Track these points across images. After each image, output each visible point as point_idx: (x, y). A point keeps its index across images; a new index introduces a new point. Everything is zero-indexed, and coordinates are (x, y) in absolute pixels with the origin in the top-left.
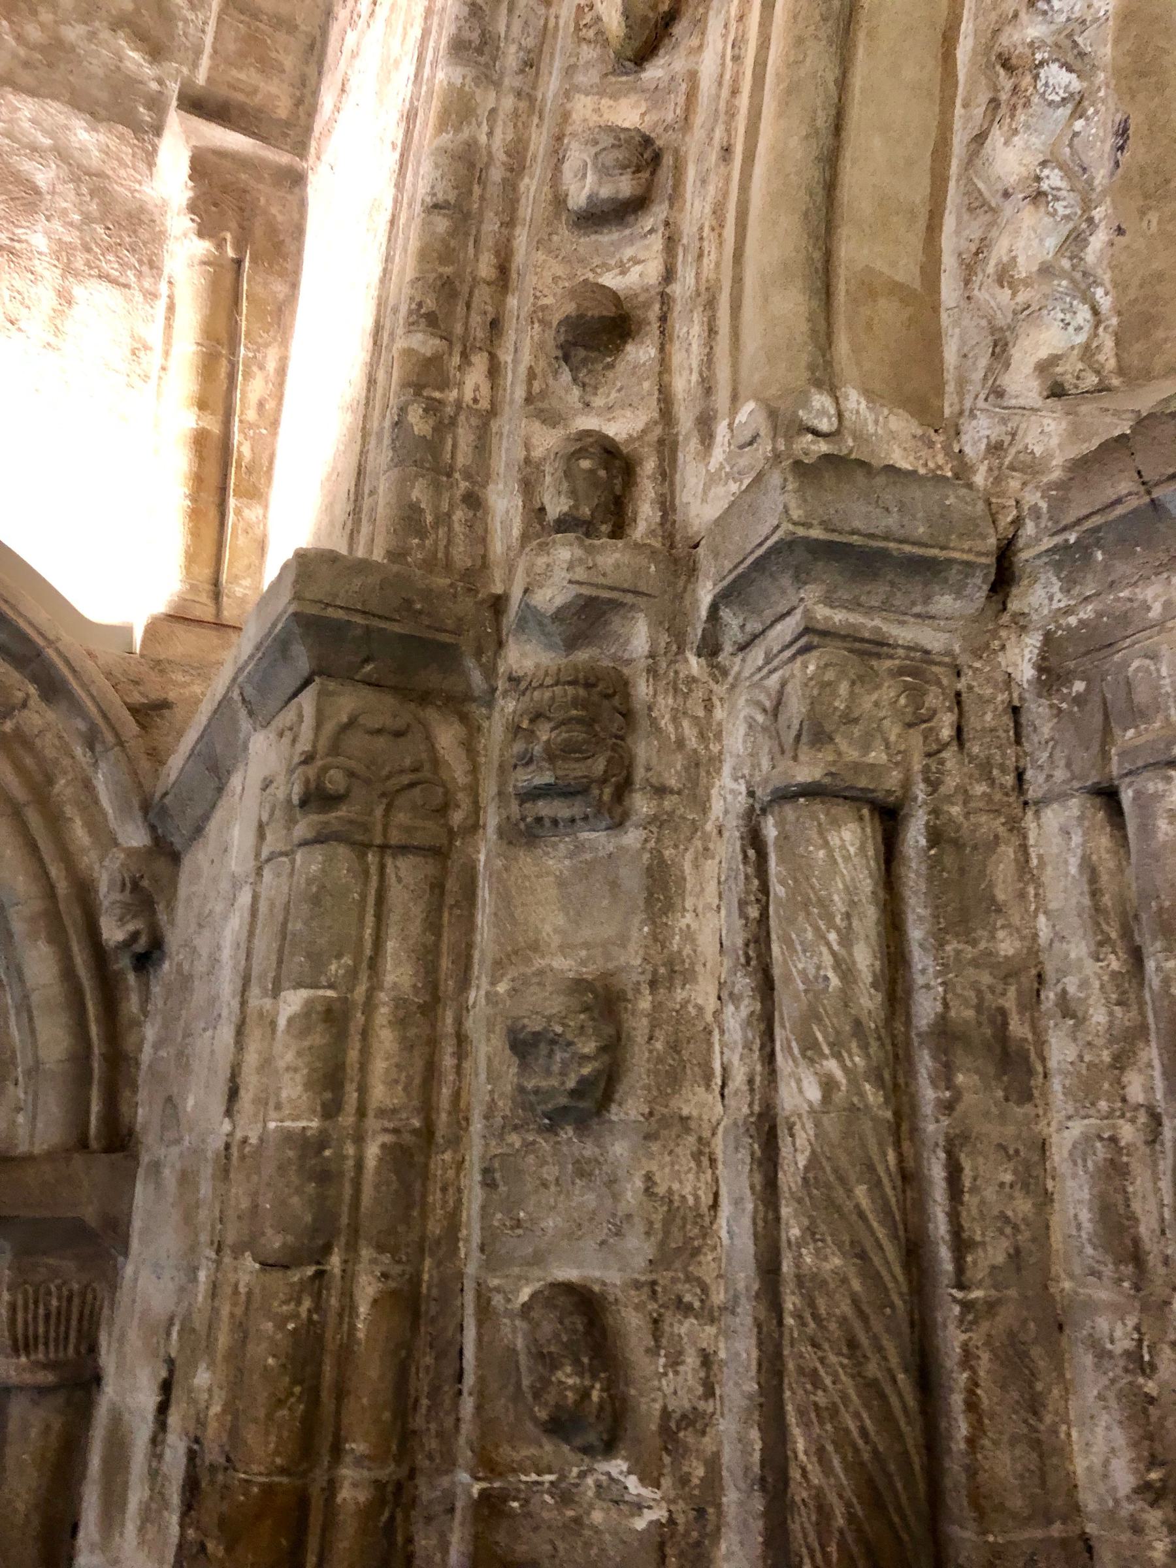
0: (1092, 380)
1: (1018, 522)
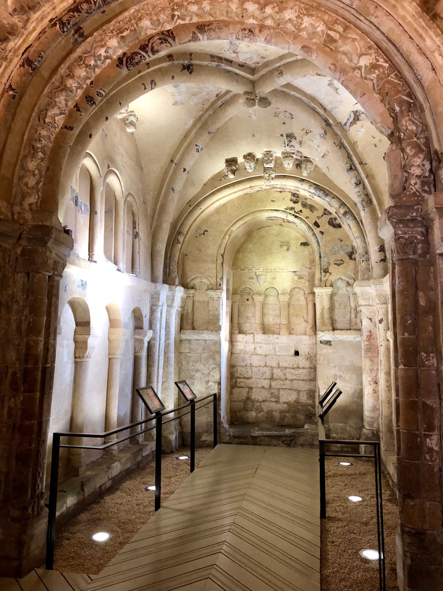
0: (36, 208)
1: (23, 231)
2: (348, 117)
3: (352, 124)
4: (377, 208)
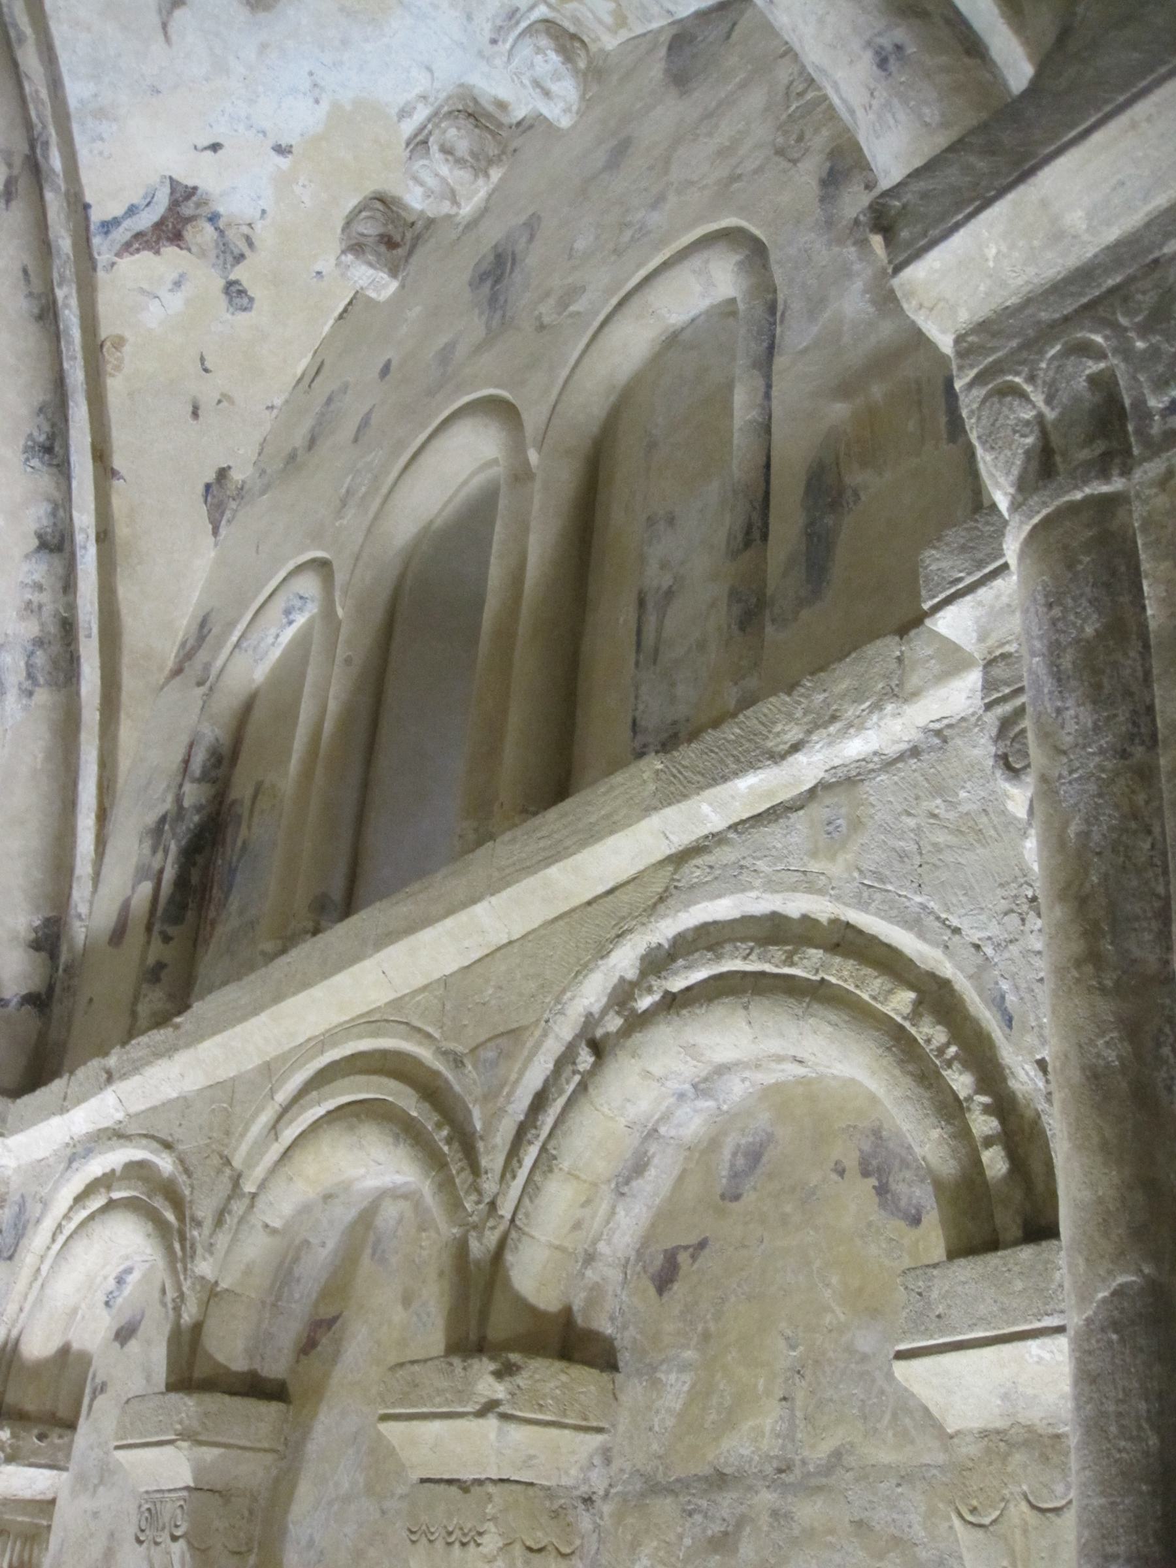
2: (136, 199)
3: (143, 241)
4: (91, 715)
